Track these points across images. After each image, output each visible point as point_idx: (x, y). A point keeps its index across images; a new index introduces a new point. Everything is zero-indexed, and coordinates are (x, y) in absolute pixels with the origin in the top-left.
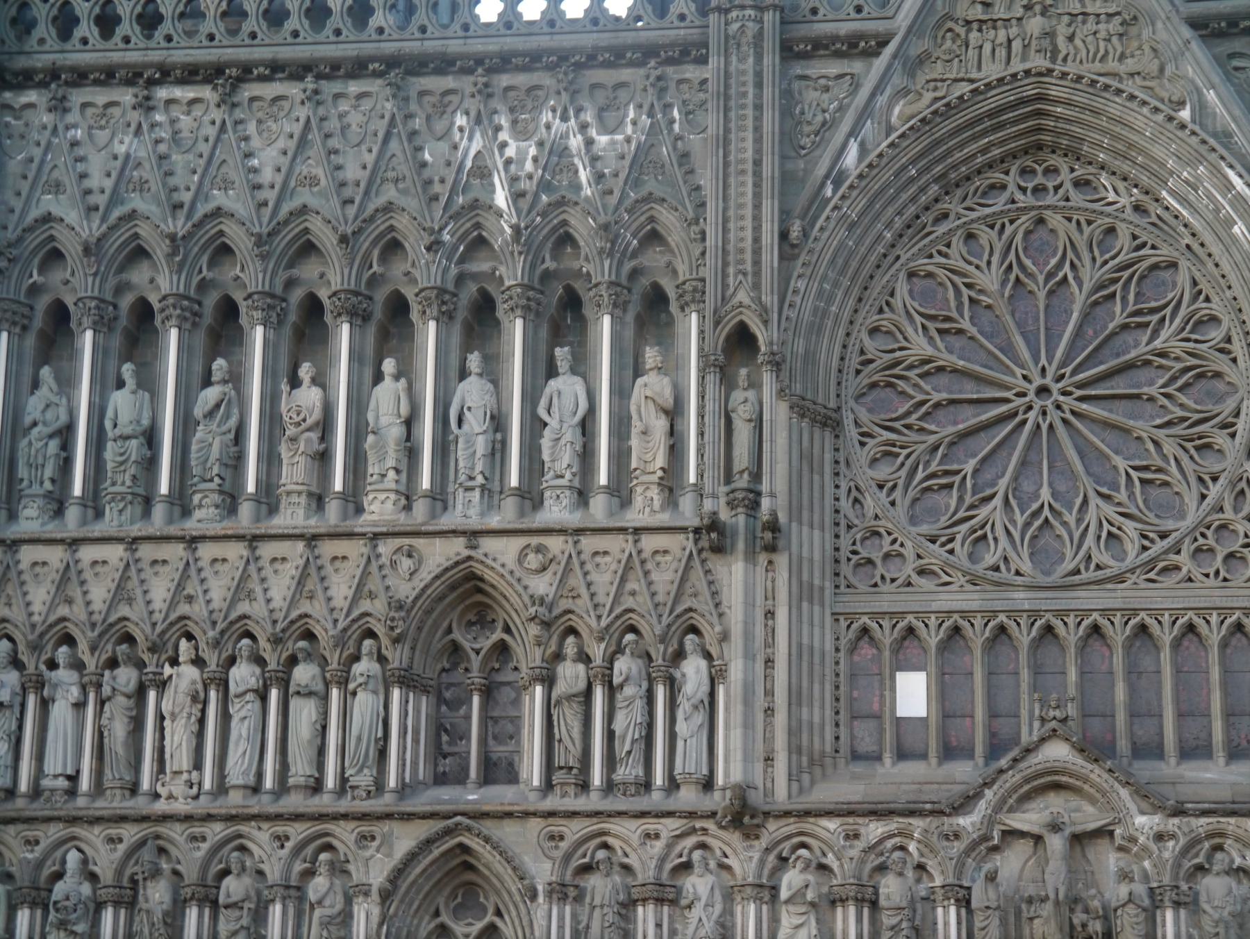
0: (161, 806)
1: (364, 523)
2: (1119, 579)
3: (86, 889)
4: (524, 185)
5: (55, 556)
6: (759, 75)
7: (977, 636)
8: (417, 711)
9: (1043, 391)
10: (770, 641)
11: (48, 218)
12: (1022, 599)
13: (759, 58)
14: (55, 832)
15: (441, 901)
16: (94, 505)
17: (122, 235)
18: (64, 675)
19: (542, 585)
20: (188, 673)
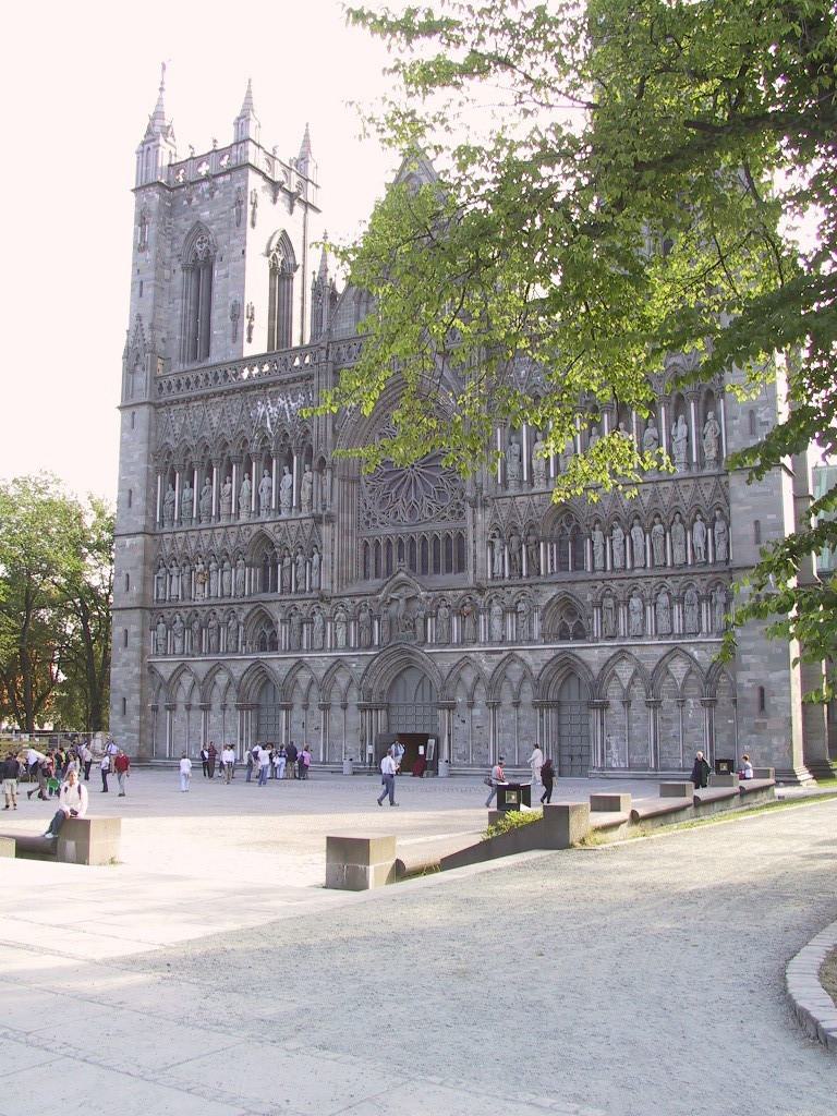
0: (196, 603)
1: (238, 523)
2: (430, 521)
3: (181, 625)
4: (275, 420)
5: (170, 536)
6: (326, 382)
7: (394, 540)
8: (255, 573)
9: (413, 466)
10: (333, 549)
11: (167, 443)
12: (405, 530)
13: (326, 378)
14: (172, 611)
15: (262, 624)
16: (180, 522)
17: (183, 446)
18: (175, 569)
19: (278, 536)
20: (201, 566)
